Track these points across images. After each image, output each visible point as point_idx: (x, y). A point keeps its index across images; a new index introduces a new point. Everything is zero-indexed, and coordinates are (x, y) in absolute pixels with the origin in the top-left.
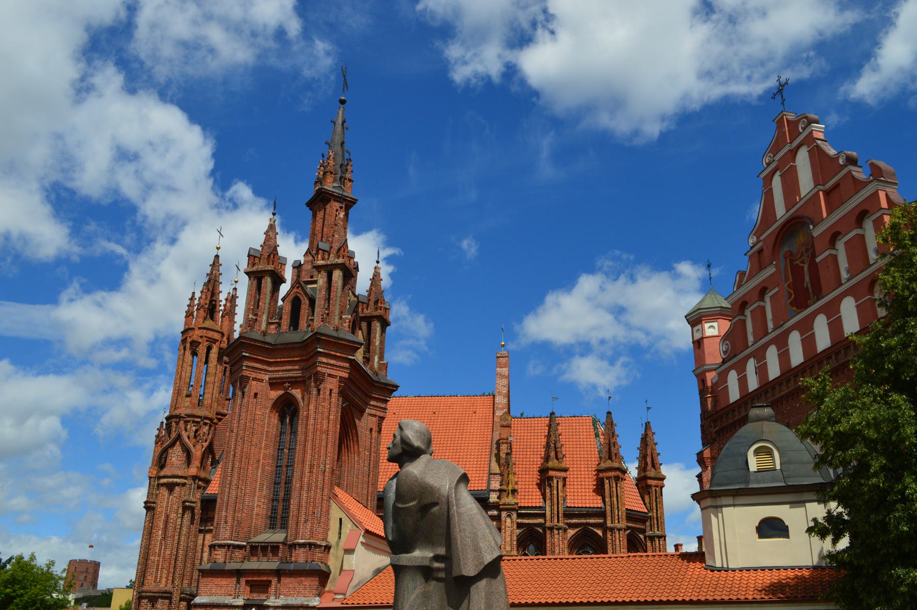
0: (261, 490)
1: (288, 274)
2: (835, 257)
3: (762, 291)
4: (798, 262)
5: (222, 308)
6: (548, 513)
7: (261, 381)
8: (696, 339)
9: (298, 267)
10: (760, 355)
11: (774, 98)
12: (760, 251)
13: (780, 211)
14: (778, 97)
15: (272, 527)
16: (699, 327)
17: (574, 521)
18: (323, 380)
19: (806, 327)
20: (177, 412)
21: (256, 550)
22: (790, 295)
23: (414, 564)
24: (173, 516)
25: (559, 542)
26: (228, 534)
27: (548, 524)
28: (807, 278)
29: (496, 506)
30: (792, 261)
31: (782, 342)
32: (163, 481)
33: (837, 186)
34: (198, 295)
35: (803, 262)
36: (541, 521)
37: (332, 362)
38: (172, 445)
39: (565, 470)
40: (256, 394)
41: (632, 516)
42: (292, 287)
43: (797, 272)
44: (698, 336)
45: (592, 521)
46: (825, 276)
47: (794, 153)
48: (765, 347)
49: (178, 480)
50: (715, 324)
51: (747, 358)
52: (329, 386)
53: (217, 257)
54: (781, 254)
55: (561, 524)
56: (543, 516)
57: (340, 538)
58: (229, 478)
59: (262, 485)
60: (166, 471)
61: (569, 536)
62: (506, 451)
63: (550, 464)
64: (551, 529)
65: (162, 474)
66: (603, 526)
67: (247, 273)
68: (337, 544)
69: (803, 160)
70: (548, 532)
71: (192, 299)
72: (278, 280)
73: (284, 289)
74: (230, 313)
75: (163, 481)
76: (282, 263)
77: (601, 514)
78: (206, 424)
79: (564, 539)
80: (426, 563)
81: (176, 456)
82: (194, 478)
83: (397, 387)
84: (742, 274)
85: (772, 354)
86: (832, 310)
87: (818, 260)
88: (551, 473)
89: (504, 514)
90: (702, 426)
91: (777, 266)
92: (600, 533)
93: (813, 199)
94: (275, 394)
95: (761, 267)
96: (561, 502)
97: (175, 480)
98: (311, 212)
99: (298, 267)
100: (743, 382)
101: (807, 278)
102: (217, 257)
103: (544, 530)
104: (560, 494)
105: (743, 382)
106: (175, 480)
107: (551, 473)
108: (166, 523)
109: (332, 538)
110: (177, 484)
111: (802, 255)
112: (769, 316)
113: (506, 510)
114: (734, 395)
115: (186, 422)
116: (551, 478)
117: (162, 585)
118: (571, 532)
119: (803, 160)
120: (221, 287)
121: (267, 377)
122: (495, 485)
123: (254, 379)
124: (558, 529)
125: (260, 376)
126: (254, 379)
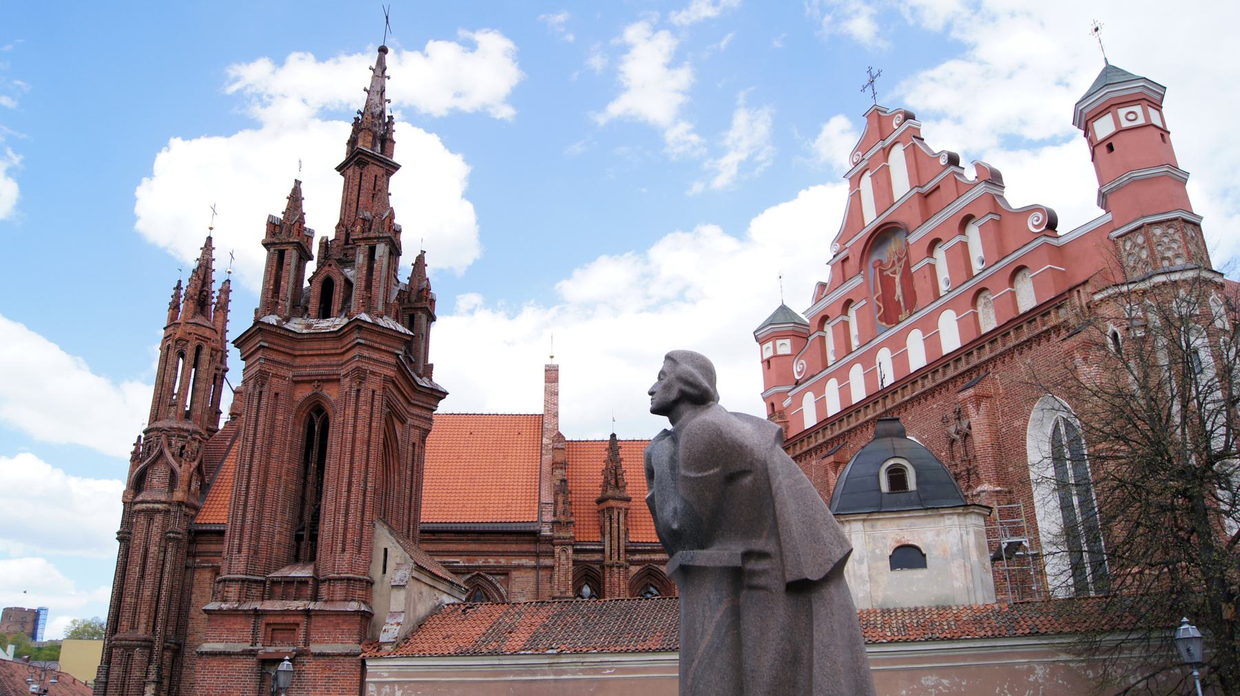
0: (283, 512)
1: (315, 250)
2: (932, 267)
3: (848, 304)
4: (888, 273)
5: (215, 300)
6: (607, 549)
7: (284, 378)
8: (765, 357)
9: (325, 245)
14: (869, 90)
15: (296, 559)
16: (770, 344)
17: (638, 557)
18: (364, 379)
20: (159, 424)
21: (272, 588)
22: (879, 308)
23: (718, 564)
24: (153, 549)
25: (617, 582)
26: (242, 567)
27: (608, 562)
28: (899, 290)
29: (550, 540)
30: (881, 272)
31: (868, 360)
32: (138, 507)
34: (184, 285)
35: (894, 273)
36: (597, 557)
37: (376, 356)
39: (629, 500)
40: (277, 394)
42: (320, 265)
43: (887, 283)
44: (768, 354)
46: (921, 286)
47: (886, 152)
48: (849, 366)
49: (160, 506)
50: (788, 342)
51: (828, 378)
52: (372, 387)
53: (209, 239)
55: (622, 561)
56: (603, 551)
57: (384, 572)
58: (243, 498)
59: (284, 507)
61: (631, 574)
62: (560, 477)
63: (610, 493)
64: (611, 567)
65: (140, 498)
67: (266, 245)
68: (382, 581)
69: (898, 160)
70: (607, 570)
71: (179, 287)
72: (305, 256)
73: (311, 267)
74: (223, 307)
75: (138, 507)
76: (309, 236)
78: (194, 439)
79: (626, 578)
80: (737, 562)
81: (158, 478)
82: (180, 504)
83: (446, 394)
84: (822, 286)
88: (612, 503)
89: (557, 549)
91: (864, 277)
93: (907, 203)
94: (303, 393)
96: (622, 536)
97: (156, 506)
98: (342, 179)
99: (325, 245)
101: (899, 290)
102: (209, 239)
103: (603, 568)
104: (622, 527)
106: (156, 506)
107: (612, 503)
109: (376, 572)
110: (158, 511)
111: (894, 264)
112: (854, 330)
113: (561, 544)
114: (810, 420)
116: (611, 509)
118: (634, 569)
119: (898, 160)
120: (214, 276)
122: (548, 517)
123: (275, 375)
124: (619, 567)
125: (282, 372)
126: (275, 375)
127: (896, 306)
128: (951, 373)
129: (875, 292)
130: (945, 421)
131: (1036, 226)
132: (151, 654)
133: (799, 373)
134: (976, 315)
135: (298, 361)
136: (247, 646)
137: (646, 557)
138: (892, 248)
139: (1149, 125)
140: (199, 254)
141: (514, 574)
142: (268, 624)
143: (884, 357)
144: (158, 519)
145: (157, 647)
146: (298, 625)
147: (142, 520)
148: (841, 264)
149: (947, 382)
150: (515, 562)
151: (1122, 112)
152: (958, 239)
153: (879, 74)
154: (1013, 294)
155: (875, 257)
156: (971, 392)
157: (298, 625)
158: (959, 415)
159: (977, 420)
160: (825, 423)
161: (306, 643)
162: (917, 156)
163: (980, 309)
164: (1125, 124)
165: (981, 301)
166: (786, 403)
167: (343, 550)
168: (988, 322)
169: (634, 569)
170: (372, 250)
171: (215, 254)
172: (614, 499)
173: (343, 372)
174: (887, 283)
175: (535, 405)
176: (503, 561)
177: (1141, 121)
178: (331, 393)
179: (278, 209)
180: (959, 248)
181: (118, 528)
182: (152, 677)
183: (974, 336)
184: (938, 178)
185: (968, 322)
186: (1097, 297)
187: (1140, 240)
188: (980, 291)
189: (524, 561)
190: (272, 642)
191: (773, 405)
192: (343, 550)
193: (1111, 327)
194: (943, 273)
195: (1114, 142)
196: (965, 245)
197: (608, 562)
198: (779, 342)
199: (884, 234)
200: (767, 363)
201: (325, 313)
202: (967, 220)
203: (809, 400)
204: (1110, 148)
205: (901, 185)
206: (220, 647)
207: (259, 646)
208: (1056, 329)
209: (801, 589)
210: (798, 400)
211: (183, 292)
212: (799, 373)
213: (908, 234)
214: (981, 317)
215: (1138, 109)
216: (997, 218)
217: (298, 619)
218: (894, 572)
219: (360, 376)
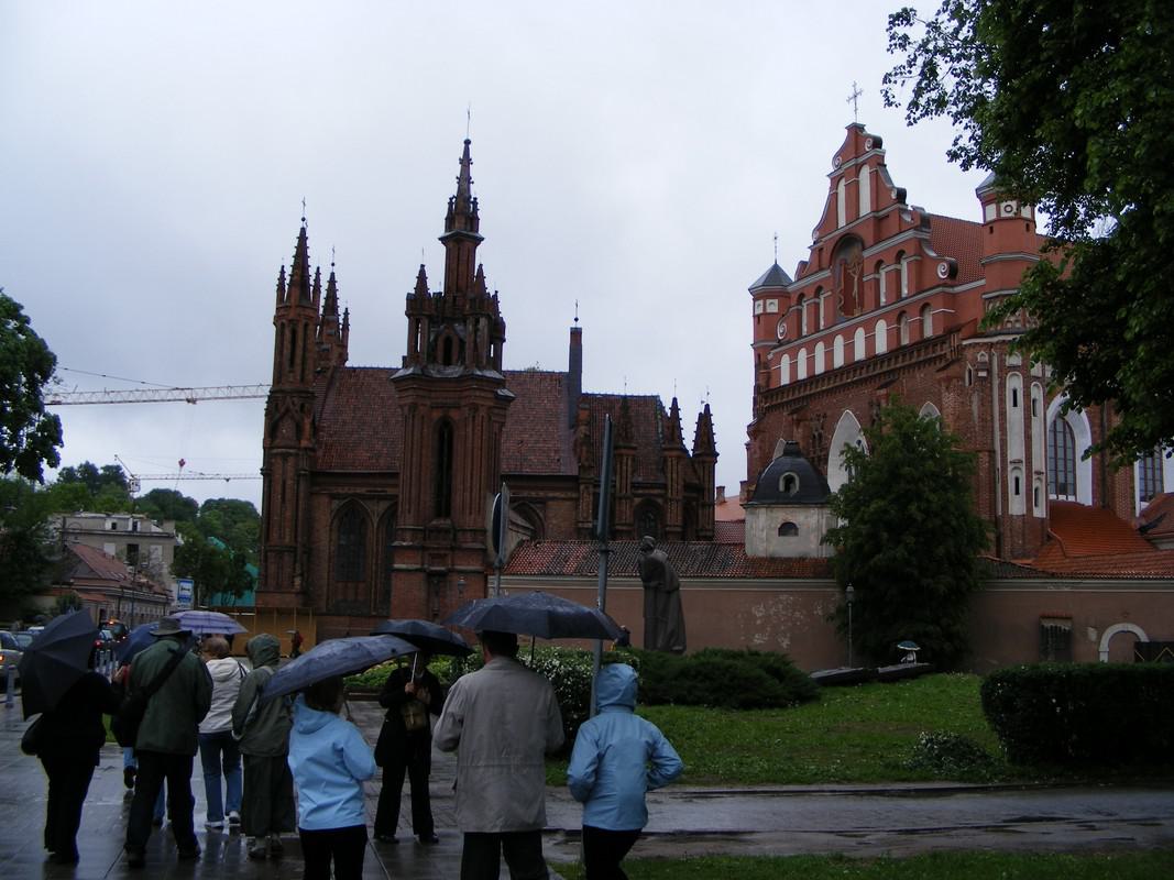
2: (877, 281)
11: (848, 101)
12: (821, 250)
13: (842, 222)
15: (439, 515)
16: (761, 302)
17: (640, 492)
19: (849, 335)
24: (289, 482)
28: (856, 289)
32: (275, 451)
34: (288, 270)
38: (281, 418)
41: (687, 487)
44: (759, 311)
45: (656, 492)
47: (858, 168)
48: (816, 341)
50: (776, 301)
51: (800, 347)
54: (838, 261)
60: (277, 441)
61: (634, 504)
63: (621, 443)
64: (620, 499)
70: (617, 501)
71: (283, 272)
75: (275, 451)
79: (631, 506)
82: (306, 449)
86: (869, 327)
87: (864, 279)
90: (754, 398)
91: (833, 271)
92: (660, 501)
94: (437, 415)
100: (794, 367)
101: (856, 289)
105: (794, 367)
107: (623, 451)
110: (291, 454)
114: (785, 380)
115: (292, 397)
116: (622, 455)
117: (287, 540)
118: (637, 500)
119: (865, 172)
120: (310, 262)
121: (428, 403)
126: (422, 405)
127: (851, 303)
129: (839, 286)
130: (871, 405)
131: (943, 274)
132: (295, 556)
133: (782, 335)
134: (899, 329)
135: (433, 395)
136: (419, 566)
137: (647, 491)
138: (856, 250)
140: (296, 243)
141: (550, 503)
142: (430, 554)
144: (291, 461)
145: (299, 551)
146: (446, 555)
147: (280, 461)
148: (817, 250)
149: (875, 376)
150: (551, 495)
152: (892, 267)
153: (860, 93)
155: (842, 257)
157: (446, 555)
160: (796, 384)
161: (453, 565)
164: (1004, 215)
165: (904, 319)
166: (770, 357)
167: (471, 513)
168: (905, 341)
169: (637, 500)
170: (477, 322)
172: (625, 448)
173: (463, 403)
174: (848, 280)
175: (563, 366)
176: (541, 494)
178: (454, 414)
179: (410, 286)
180: (894, 274)
181: (261, 465)
185: (894, 335)
186: (965, 343)
188: (902, 313)
190: (432, 565)
191: (759, 356)
192: (471, 513)
193: (969, 366)
195: (995, 226)
197: (618, 494)
198: (768, 301)
199: (848, 241)
200: (757, 318)
201: (447, 362)
202: (900, 255)
203: (786, 360)
205: (866, 207)
206: (404, 566)
207: (426, 566)
211: (287, 281)
212: (782, 335)
213: (864, 249)
214: (902, 330)
216: (919, 258)
217: (447, 552)
218: (782, 538)
219: (475, 408)
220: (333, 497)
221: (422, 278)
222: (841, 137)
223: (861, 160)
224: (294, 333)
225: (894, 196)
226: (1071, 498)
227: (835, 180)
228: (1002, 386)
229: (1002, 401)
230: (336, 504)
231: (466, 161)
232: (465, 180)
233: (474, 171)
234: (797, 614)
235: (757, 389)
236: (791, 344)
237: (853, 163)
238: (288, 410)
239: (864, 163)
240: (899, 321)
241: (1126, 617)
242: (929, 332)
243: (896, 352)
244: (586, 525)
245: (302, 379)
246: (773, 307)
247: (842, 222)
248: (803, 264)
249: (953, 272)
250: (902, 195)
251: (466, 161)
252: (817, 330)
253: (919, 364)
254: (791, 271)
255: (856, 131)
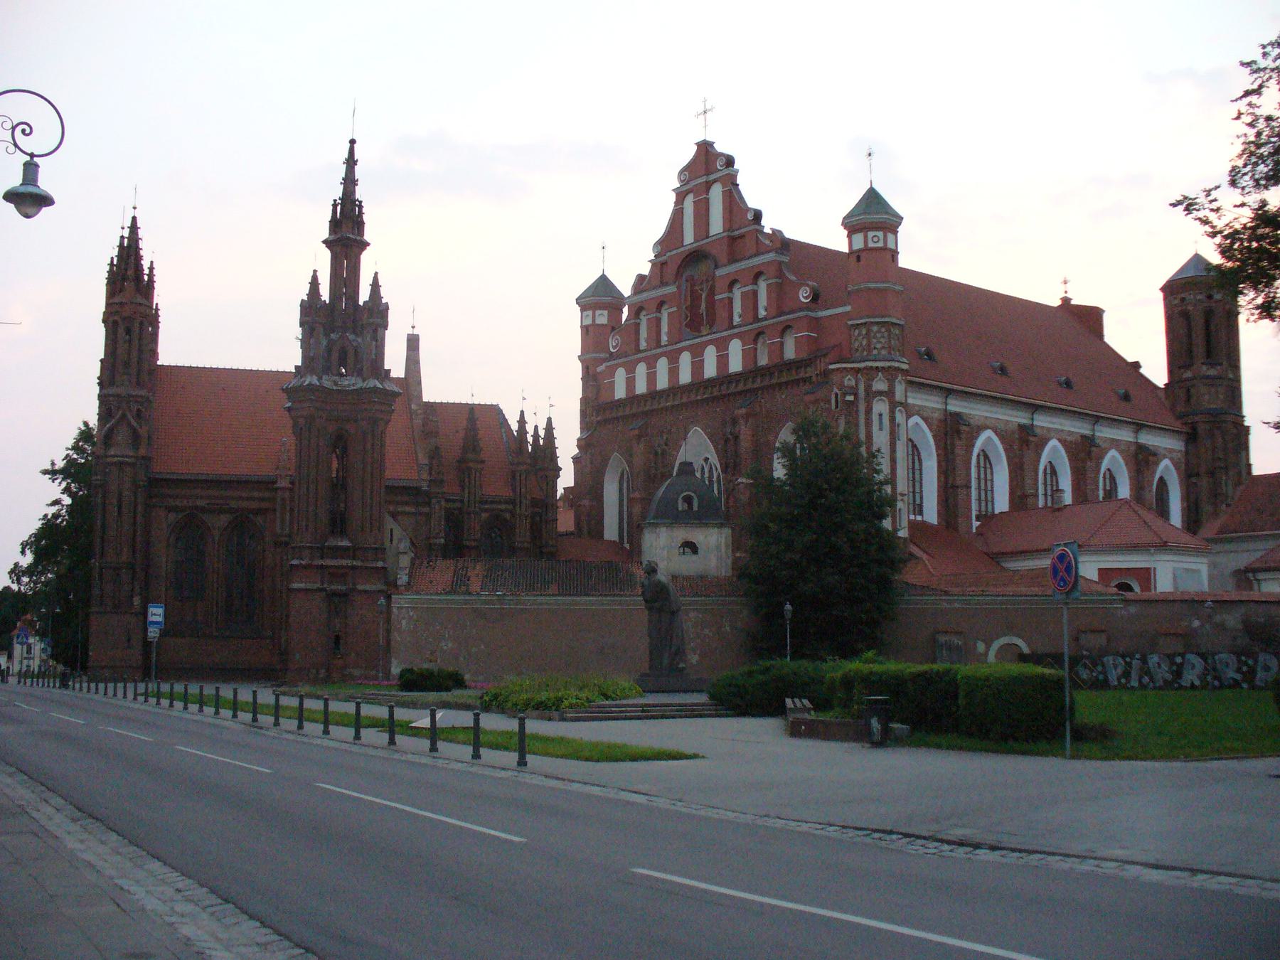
2: (731, 300)
3: (661, 305)
6: (466, 500)
10: (651, 363)
12: (663, 264)
13: (689, 238)
16: (590, 313)
19: (697, 352)
21: (324, 552)
28: (703, 305)
29: (427, 494)
31: (674, 359)
32: (109, 460)
33: (742, 236)
36: (457, 505)
39: (483, 462)
43: (695, 298)
44: (588, 322)
45: (503, 507)
46: (721, 314)
47: (708, 185)
50: (606, 313)
51: (639, 361)
53: (134, 219)
56: (462, 501)
66: (512, 513)
69: (716, 193)
77: (513, 502)
85: (662, 365)
86: (722, 345)
89: (434, 501)
92: (508, 516)
95: (663, 283)
100: (630, 383)
101: (703, 305)
102: (134, 219)
105: (630, 383)
108: (120, 500)
109: (387, 543)
110: (129, 464)
112: (665, 328)
114: (620, 393)
116: (469, 469)
118: (484, 515)
119: (716, 193)
127: (699, 317)
128: (732, 389)
133: (614, 347)
134: (756, 349)
138: (704, 267)
139: (885, 249)
143: (686, 359)
144: (128, 470)
151: (871, 234)
152: (750, 288)
154: (782, 344)
155: (688, 273)
156: (743, 411)
158: (734, 422)
159: (745, 431)
160: (632, 399)
161: (354, 584)
162: (733, 197)
163: (759, 345)
164: (871, 245)
165: (760, 340)
168: (763, 361)
169: (484, 515)
171: (141, 233)
174: (695, 298)
177: (880, 244)
182: (137, 589)
183: (751, 367)
184: (743, 221)
186: (832, 367)
187: (864, 332)
188: (760, 333)
189: (407, 509)
190: (331, 583)
193: (836, 390)
194: (737, 308)
195: (863, 256)
196: (755, 293)
198: (598, 312)
199: (695, 257)
200: (585, 329)
203: (620, 376)
204: (859, 259)
205: (717, 225)
206: (302, 585)
208: (804, 380)
209: (673, 613)
210: (611, 372)
212: (614, 347)
213: (716, 267)
215: (880, 234)
220: (170, 509)
221: (314, 283)
222: (691, 152)
223: (712, 177)
224: (128, 331)
225: (750, 216)
226: (919, 518)
227: (681, 196)
228: (869, 411)
229: (869, 424)
230: (172, 517)
231: (351, 162)
232: (350, 182)
233: (359, 172)
234: (706, 631)
235: (584, 401)
236: (629, 355)
237: (702, 180)
238: (124, 416)
239: (715, 181)
240: (755, 341)
241: (1011, 629)
242: (790, 353)
243: (753, 372)
244: (437, 541)
245: (138, 384)
246: (603, 318)
247: (689, 238)
248: (641, 278)
249: (815, 297)
250: (758, 215)
251: (351, 162)
252: (658, 345)
253: (780, 385)
254: (626, 288)
255: (705, 149)
